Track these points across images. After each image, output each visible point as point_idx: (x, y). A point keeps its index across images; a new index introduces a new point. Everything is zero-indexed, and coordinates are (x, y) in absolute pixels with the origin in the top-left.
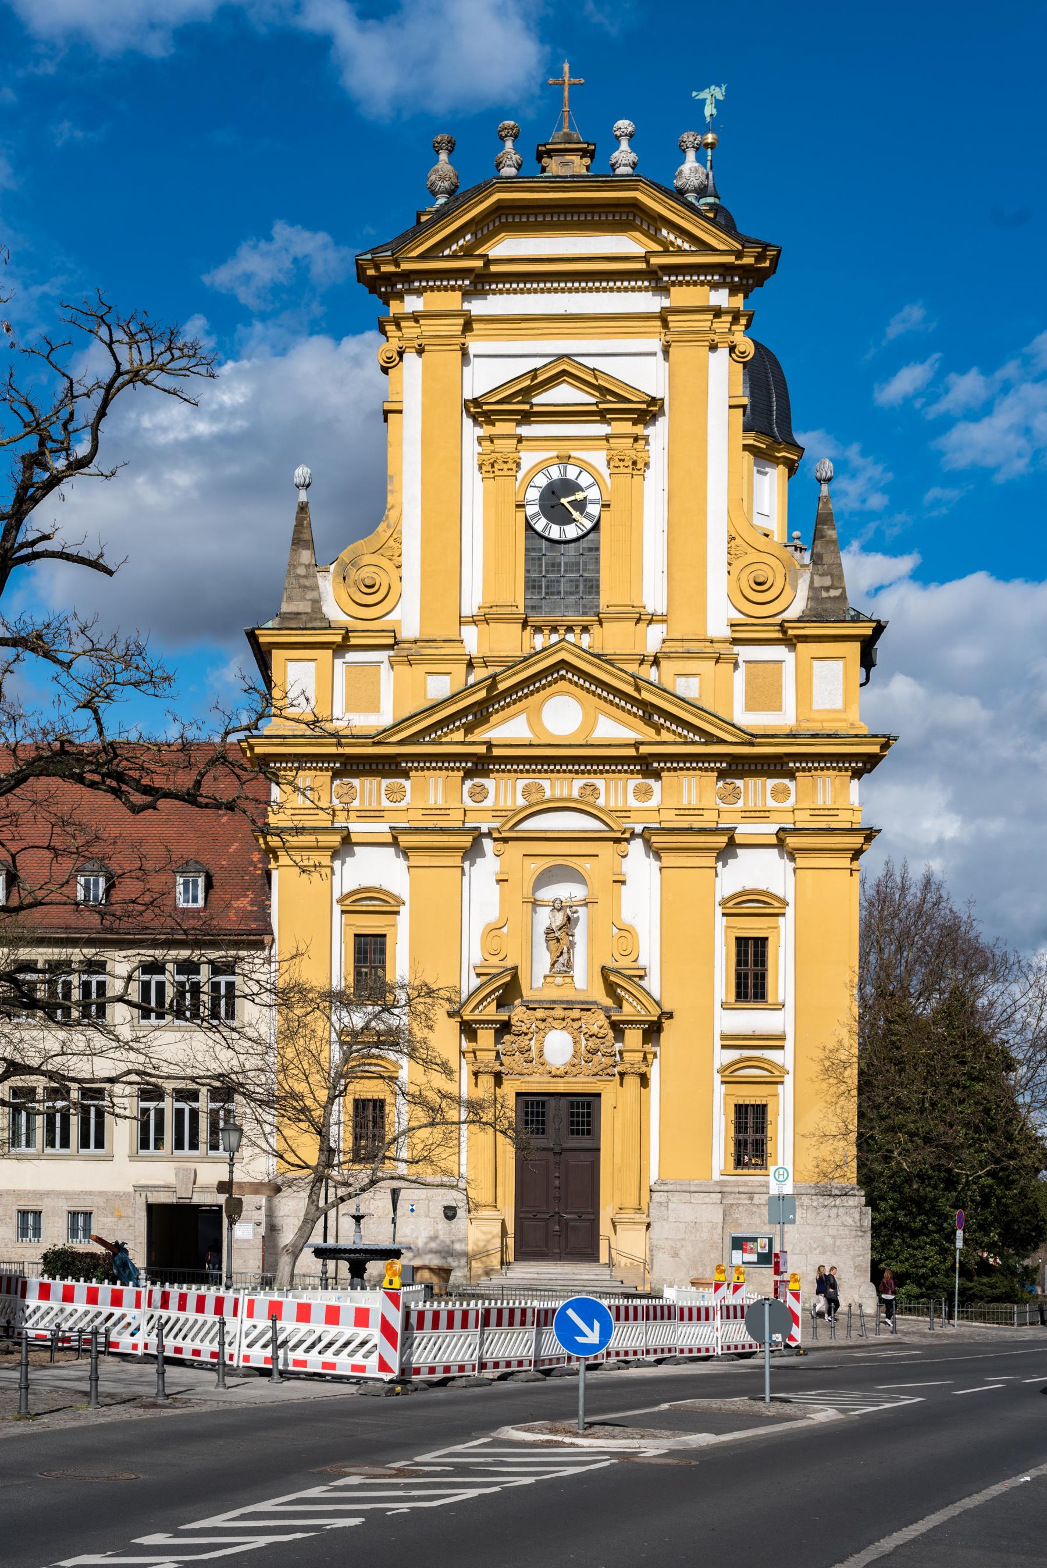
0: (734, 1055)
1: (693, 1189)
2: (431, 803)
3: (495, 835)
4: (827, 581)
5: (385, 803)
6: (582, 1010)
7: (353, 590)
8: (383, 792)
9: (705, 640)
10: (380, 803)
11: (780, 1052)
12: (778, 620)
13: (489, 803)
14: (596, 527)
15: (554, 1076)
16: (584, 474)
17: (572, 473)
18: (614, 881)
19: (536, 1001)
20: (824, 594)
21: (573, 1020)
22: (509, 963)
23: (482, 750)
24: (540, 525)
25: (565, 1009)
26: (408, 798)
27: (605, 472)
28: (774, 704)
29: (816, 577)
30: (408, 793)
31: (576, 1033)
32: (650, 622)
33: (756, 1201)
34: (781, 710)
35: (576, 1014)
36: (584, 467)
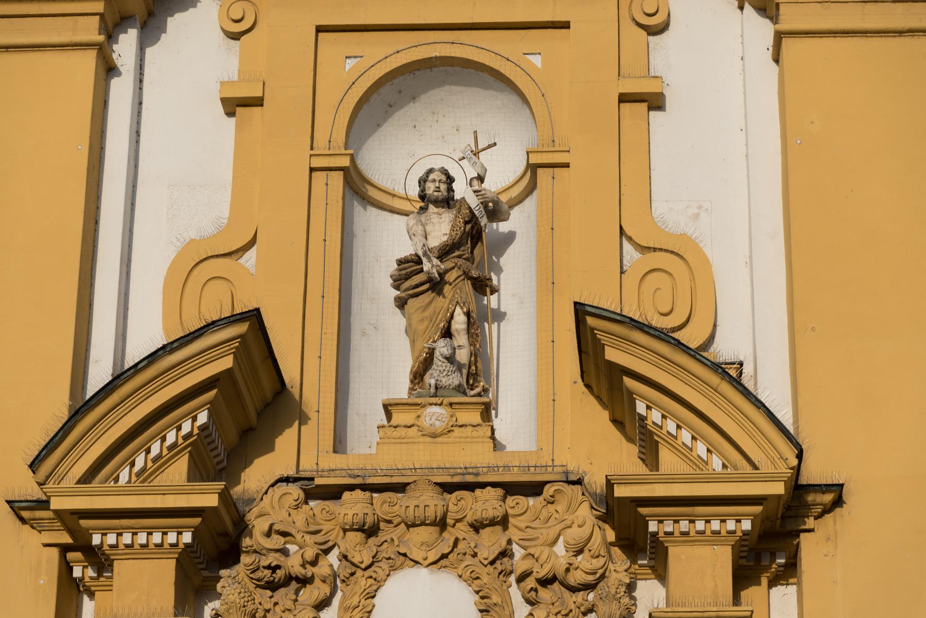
6: (511, 489)
18: (624, 98)
21: (477, 527)
31: (487, 576)
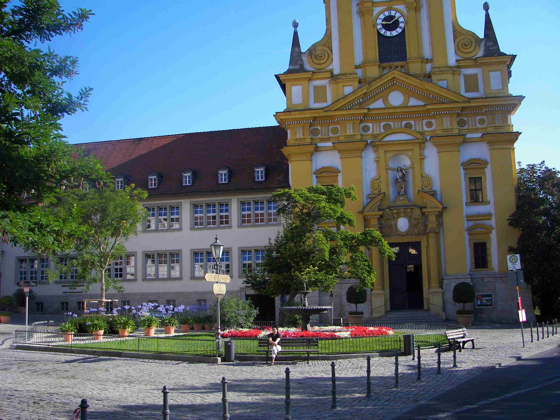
0: (471, 223)
1: (460, 277)
2: (348, 133)
3: (373, 144)
4: (491, 44)
5: (331, 135)
7: (314, 59)
8: (330, 131)
9: (448, 67)
10: (329, 135)
11: (490, 221)
12: (475, 57)
13: (370, 132)
14: (403, 31)
15: (402, 236)
16: (397, 13)
17: (393, 13)
19: (392, 207)
20: (491, 48)
22: (382, 191)
23: (366, 111)
24: (383, 32)
25: (405, 209)
26: (339, 132)
27: (404, 11)
28: (476, 89)
29: (487, 43)
30: (339, 130)
32: (426, 63)
33: (485, 281)
34: (479, 91)
35: (409, 210)
36: (397, 11)
